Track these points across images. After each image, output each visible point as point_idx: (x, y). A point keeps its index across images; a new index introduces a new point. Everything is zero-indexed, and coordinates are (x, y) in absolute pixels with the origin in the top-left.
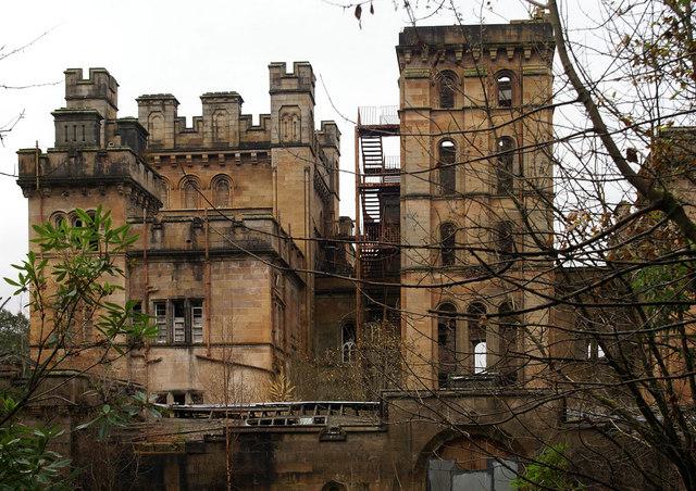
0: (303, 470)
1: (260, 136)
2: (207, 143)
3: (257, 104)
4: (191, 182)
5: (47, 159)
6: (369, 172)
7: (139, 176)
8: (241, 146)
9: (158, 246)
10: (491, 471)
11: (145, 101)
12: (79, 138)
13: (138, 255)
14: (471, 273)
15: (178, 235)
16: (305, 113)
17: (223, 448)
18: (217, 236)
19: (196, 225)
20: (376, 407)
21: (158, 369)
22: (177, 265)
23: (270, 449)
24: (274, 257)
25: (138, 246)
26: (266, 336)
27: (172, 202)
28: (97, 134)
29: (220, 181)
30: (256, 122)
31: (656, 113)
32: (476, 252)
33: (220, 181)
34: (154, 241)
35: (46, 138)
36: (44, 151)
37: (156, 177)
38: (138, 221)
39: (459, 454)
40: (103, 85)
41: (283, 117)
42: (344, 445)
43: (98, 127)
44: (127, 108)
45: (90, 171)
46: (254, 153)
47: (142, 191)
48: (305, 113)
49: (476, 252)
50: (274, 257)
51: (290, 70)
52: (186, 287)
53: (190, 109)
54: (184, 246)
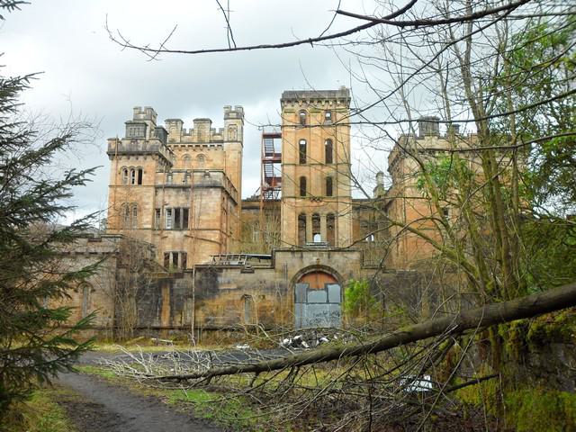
0: (232, 288)
1: (219, 138)
2: (195, 140)
3: (219, 123)
4: (187, 157)
5: (121, 143)
6: (267, 155)
7: (163, 151)
8: (210, 142)
9: (170, 183)
10: (326, 289)
11: (169, 121)
12: (136, 134)
13: (160, 187)
14: (314, 199)
15: (178, 179)
16: (239, 127)
17: (192, 276)
18: (197, 179)
19: (187, 174)
20: (269, 258)
21: (166, 241)
22: (178, 192)
23: (215, 276)
24: (223, 188)
25: (160, 183)
26: (217, 225)
27: (178, 164)
28: (145, 132)
29: (201, 157)
30: (217, 131)
31: (397, 37)
32: (367, 22)
33: (201, 157)
34: (167, 181)
35: (121, 133)
36: (120, 139)
37: (171, 153)
38: (162, 171)
39: (310, 280)
40: (152, 115)
41: (230, 130)
42: (252, 275)
43: (146, 129)
44: (161, 123)
45: (140, 149)
46: (216, 145)
47: (164, 158)
48: (239, 127)
49: (367, 22)
50: (223, 188)
51: (233, 109)
52: (181, 202)
53: (189, 125)
54: (182, 184)
